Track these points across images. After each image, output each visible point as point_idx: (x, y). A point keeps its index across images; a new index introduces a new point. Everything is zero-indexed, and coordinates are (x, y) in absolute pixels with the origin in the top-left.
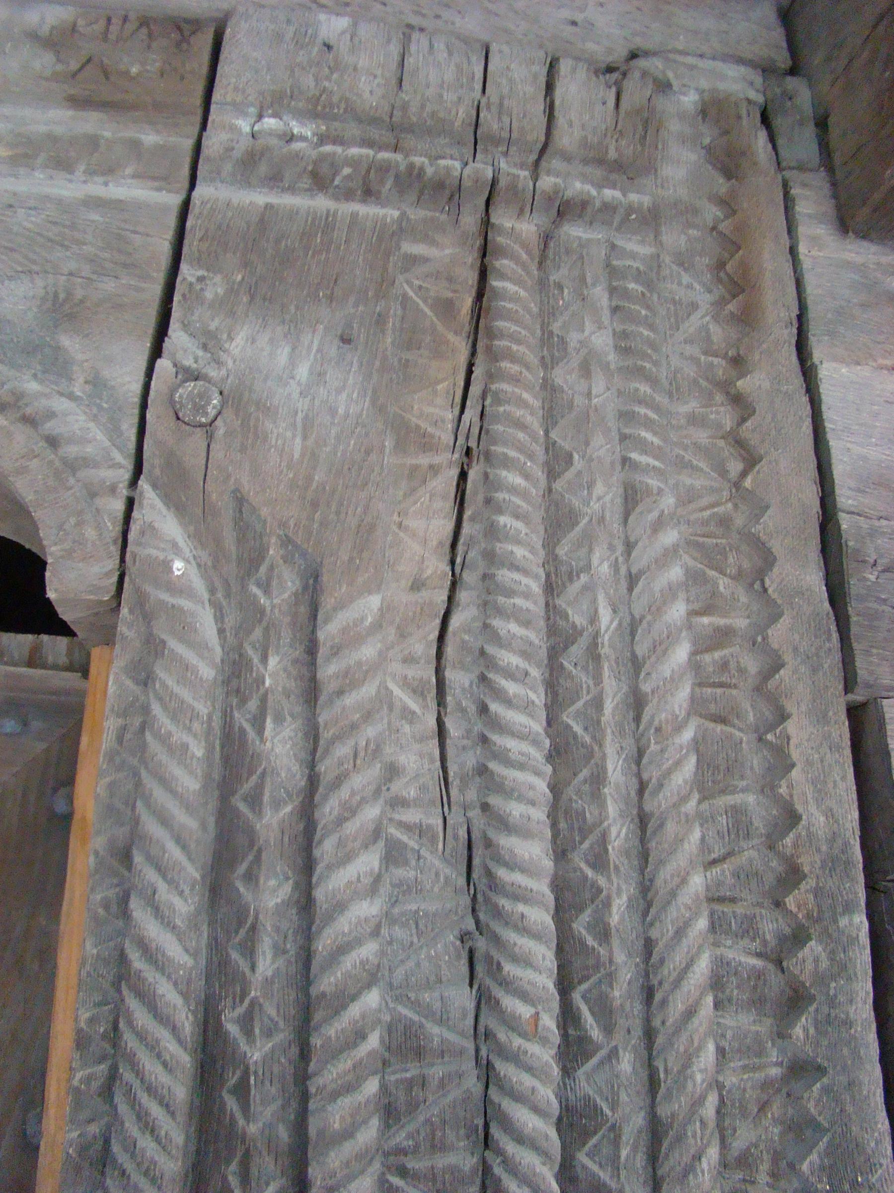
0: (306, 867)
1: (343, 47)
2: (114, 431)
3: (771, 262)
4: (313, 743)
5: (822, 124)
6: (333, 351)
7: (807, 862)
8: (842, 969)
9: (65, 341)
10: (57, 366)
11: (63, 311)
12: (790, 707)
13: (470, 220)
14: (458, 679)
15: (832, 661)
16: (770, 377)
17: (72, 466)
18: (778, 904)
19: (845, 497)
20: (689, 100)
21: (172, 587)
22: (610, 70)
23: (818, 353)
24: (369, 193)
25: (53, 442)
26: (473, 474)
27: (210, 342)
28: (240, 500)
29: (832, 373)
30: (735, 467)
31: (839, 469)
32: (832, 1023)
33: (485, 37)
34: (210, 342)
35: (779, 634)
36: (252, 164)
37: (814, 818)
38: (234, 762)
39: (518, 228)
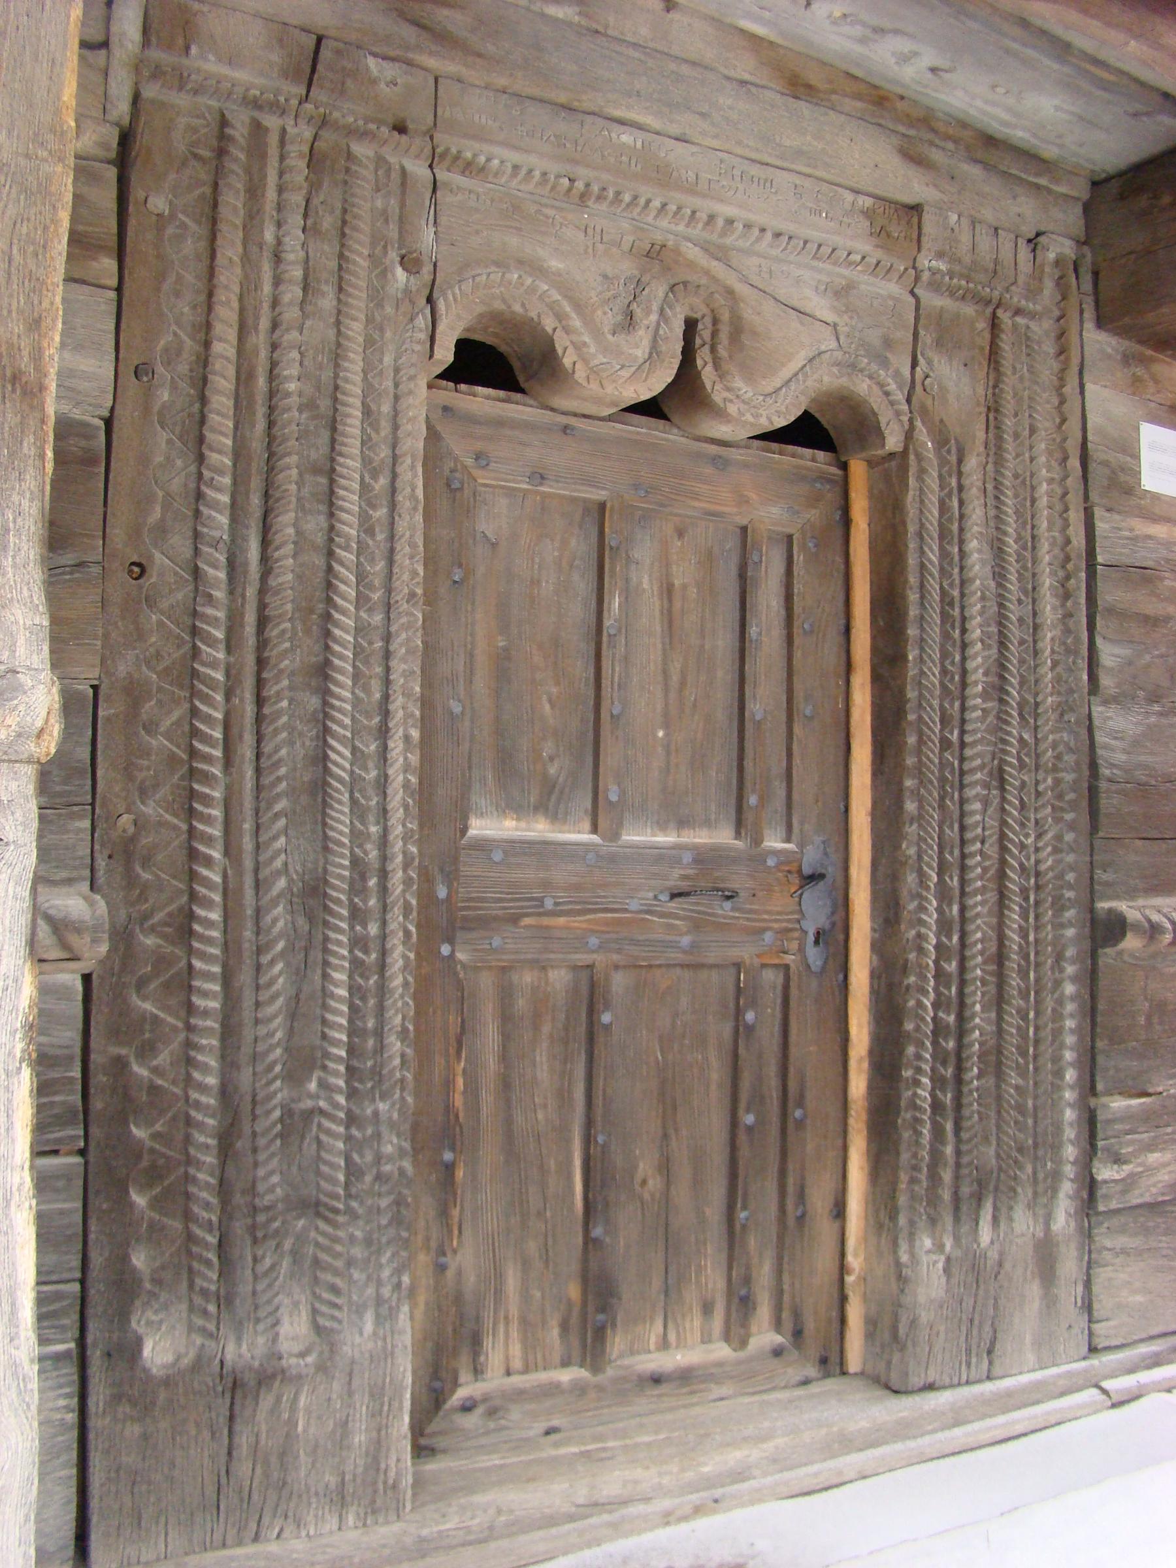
0: (961, 542)
1: (956, 228)
2: (900, 388)
3: (1074, 339)
4: (961, 503)
5: (1096, 274)
6: (962, 368)
7: (1073, 555)
8: (1079, 588)
9: (889, 355)
10: (885, 363)
11: (888, 343)
12: (1071, 506)
13: (989, 310)
14: (990, 487)
15: (1081, 492)
16: (1071, 388)
17: (892, 403)
18: (1063, 567)
19: (1090, 437)
20: (1051, 256)
21: (927, 450)
22: (1029, 241)
23: (1085, 379)
24: (963, 298)
25: (887, 394)
26: (991, 416)
27: (930, 363)
28: (941, 421)
29: (1089, 387)
30: (1058, 420)
31: (1089, 426)
32: (1077, 603)
33: (995, 224)
34: (930, 363)
35: (1069, 481)
36: (935, 287)
37: (1074, 542)
38: (943, 507)
39: (1004, 316)
